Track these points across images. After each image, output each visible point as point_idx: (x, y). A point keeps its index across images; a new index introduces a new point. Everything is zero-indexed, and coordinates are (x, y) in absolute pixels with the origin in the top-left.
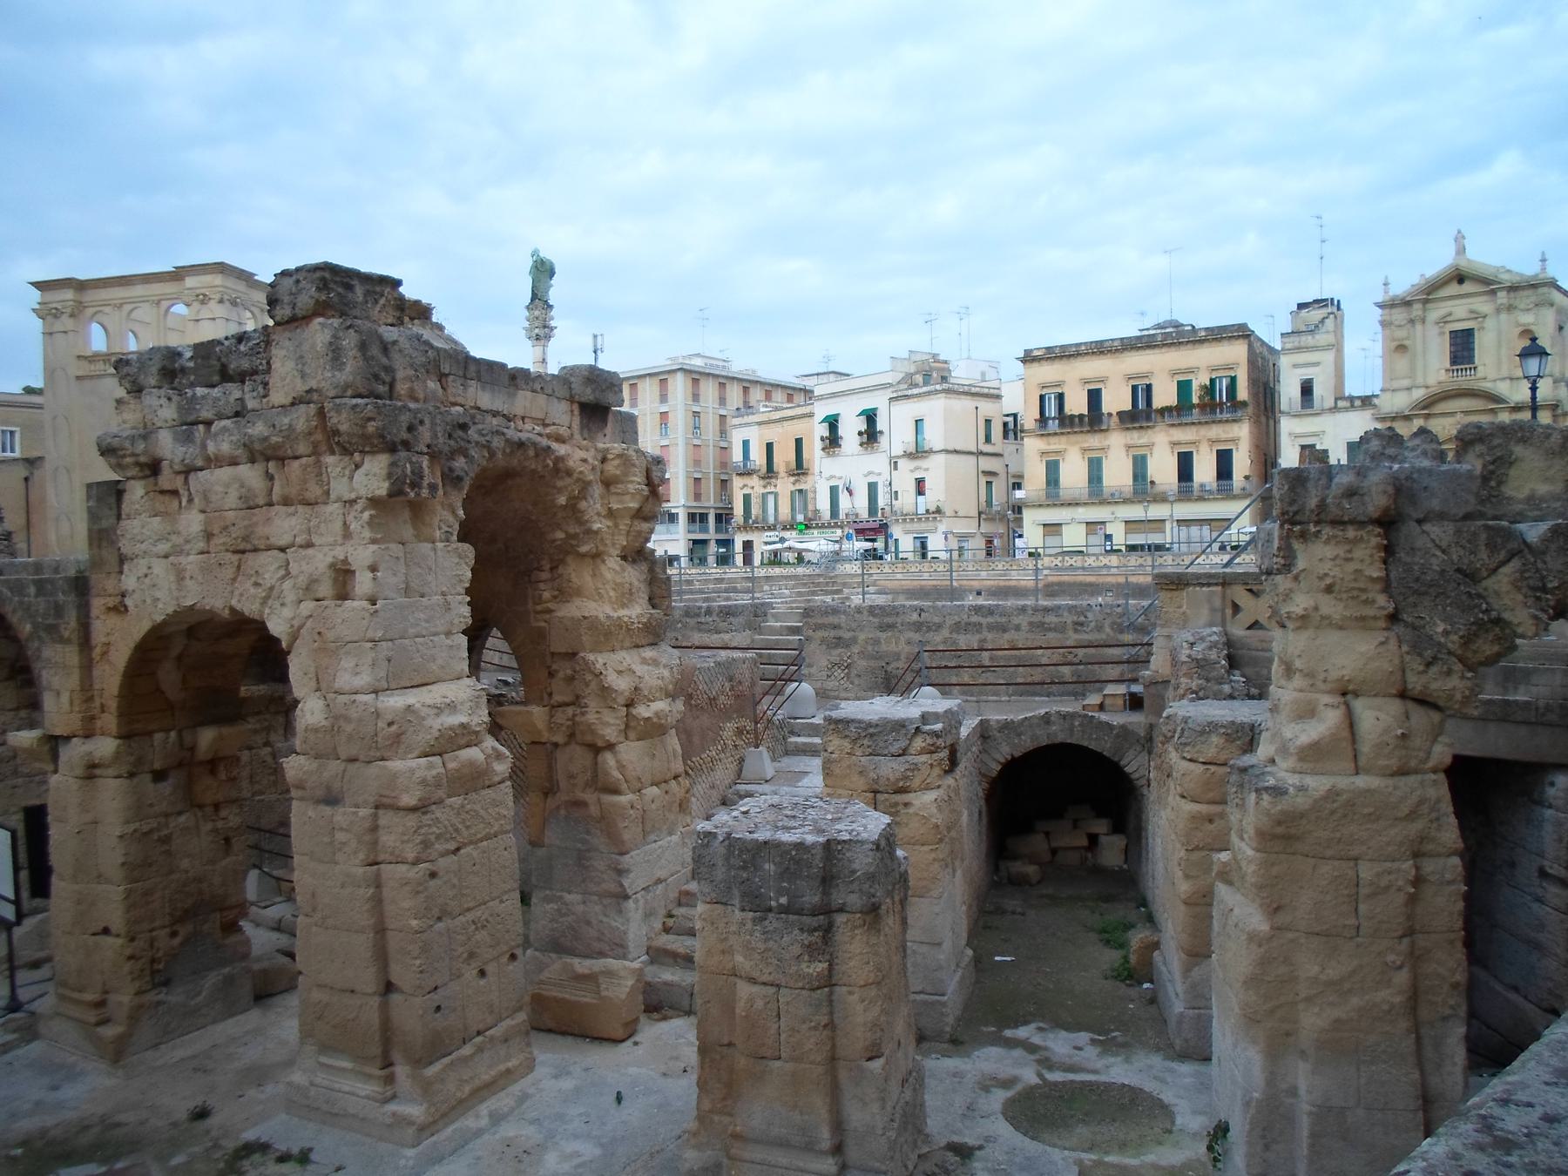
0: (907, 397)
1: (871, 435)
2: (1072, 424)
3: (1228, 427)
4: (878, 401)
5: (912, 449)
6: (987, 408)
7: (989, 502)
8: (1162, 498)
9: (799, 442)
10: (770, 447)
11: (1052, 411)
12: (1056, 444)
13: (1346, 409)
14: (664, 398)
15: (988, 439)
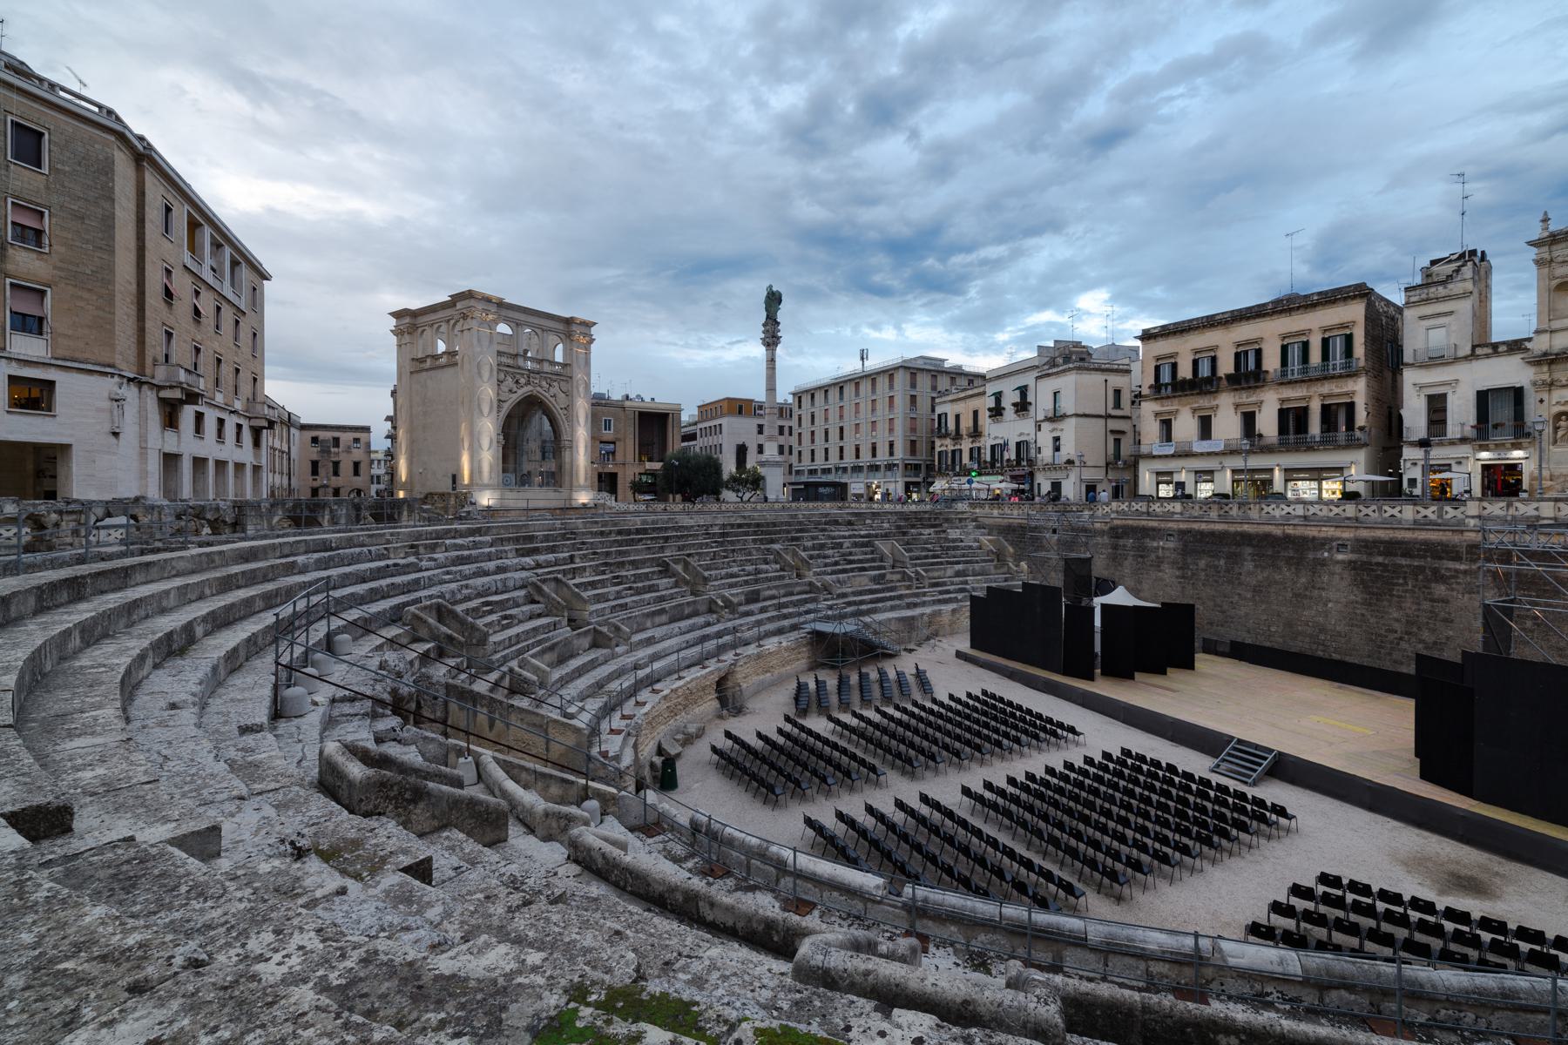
0: (1048, 375)
1: (1022, 407)
2: (1183, 390)
3: (1341, 382)
4: (1028, 379)
5: (1051, 414)
6: (1116, 381)
7: (1117, 455)
8: (1268, 450)
9: (976, 413)
10: (957, 417)
11: (1166, 378)
12: (1168, 406)
13: (1487, 356)
14: (891, 387)
15: (1117, 405)
